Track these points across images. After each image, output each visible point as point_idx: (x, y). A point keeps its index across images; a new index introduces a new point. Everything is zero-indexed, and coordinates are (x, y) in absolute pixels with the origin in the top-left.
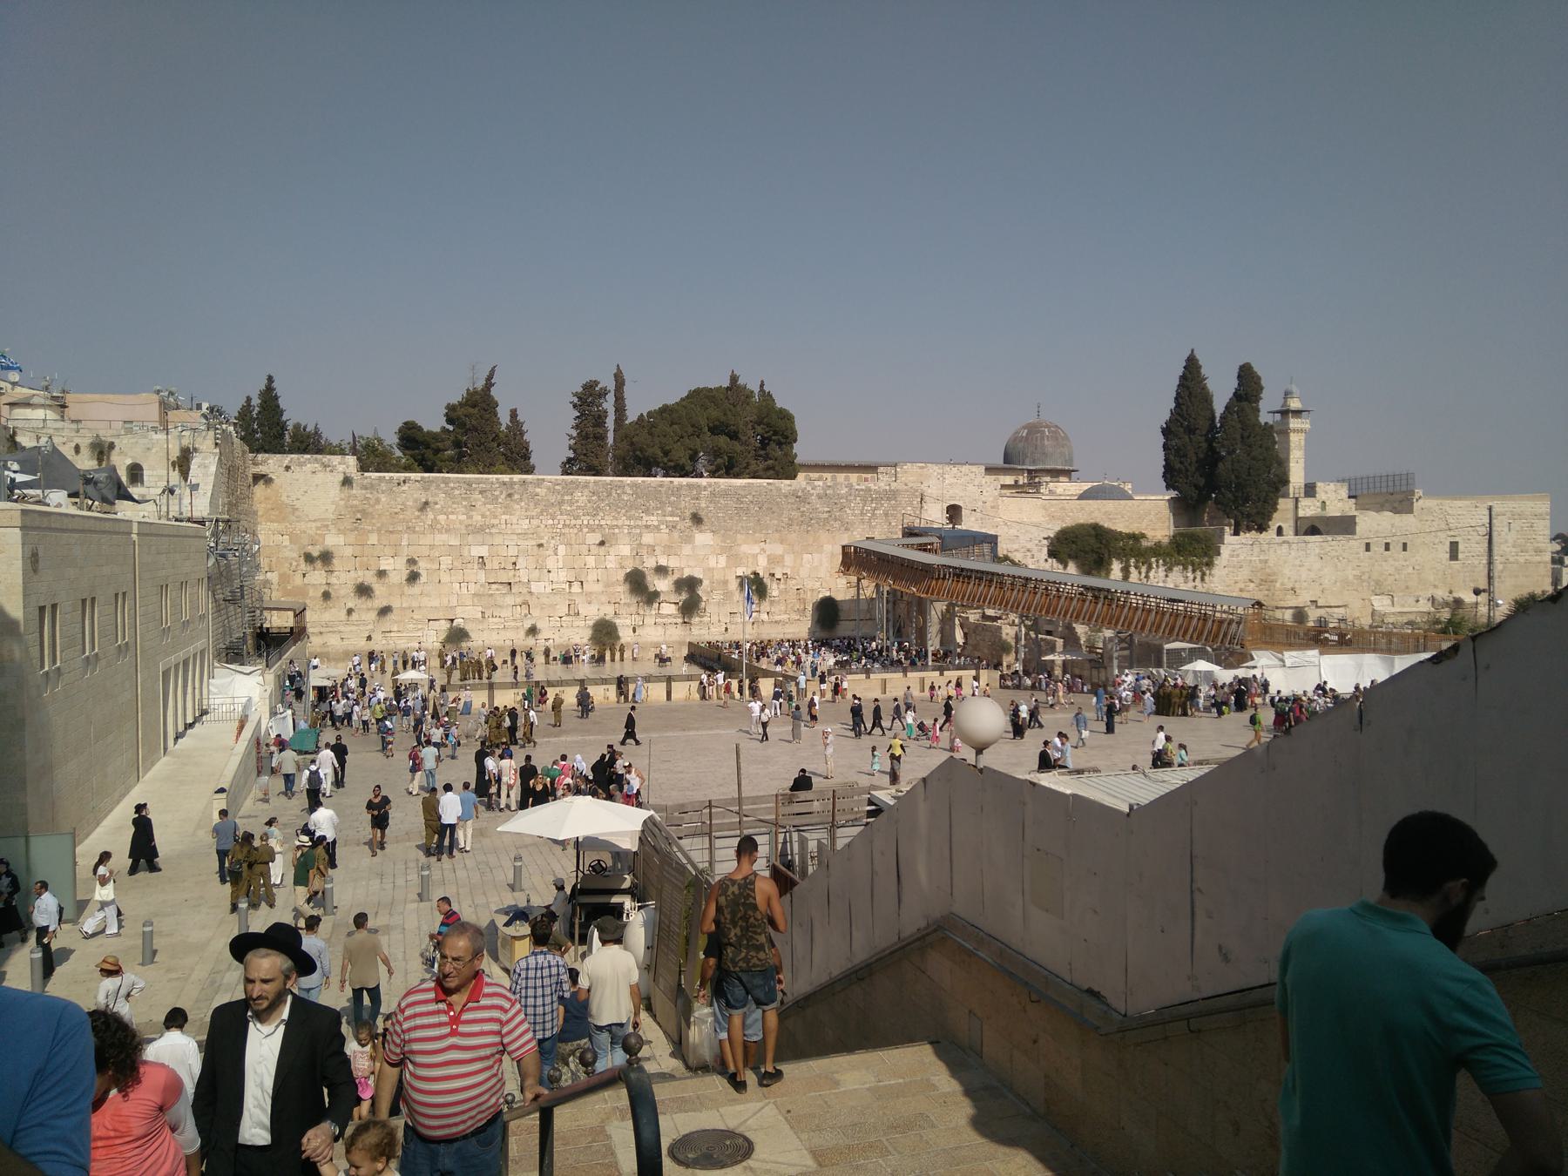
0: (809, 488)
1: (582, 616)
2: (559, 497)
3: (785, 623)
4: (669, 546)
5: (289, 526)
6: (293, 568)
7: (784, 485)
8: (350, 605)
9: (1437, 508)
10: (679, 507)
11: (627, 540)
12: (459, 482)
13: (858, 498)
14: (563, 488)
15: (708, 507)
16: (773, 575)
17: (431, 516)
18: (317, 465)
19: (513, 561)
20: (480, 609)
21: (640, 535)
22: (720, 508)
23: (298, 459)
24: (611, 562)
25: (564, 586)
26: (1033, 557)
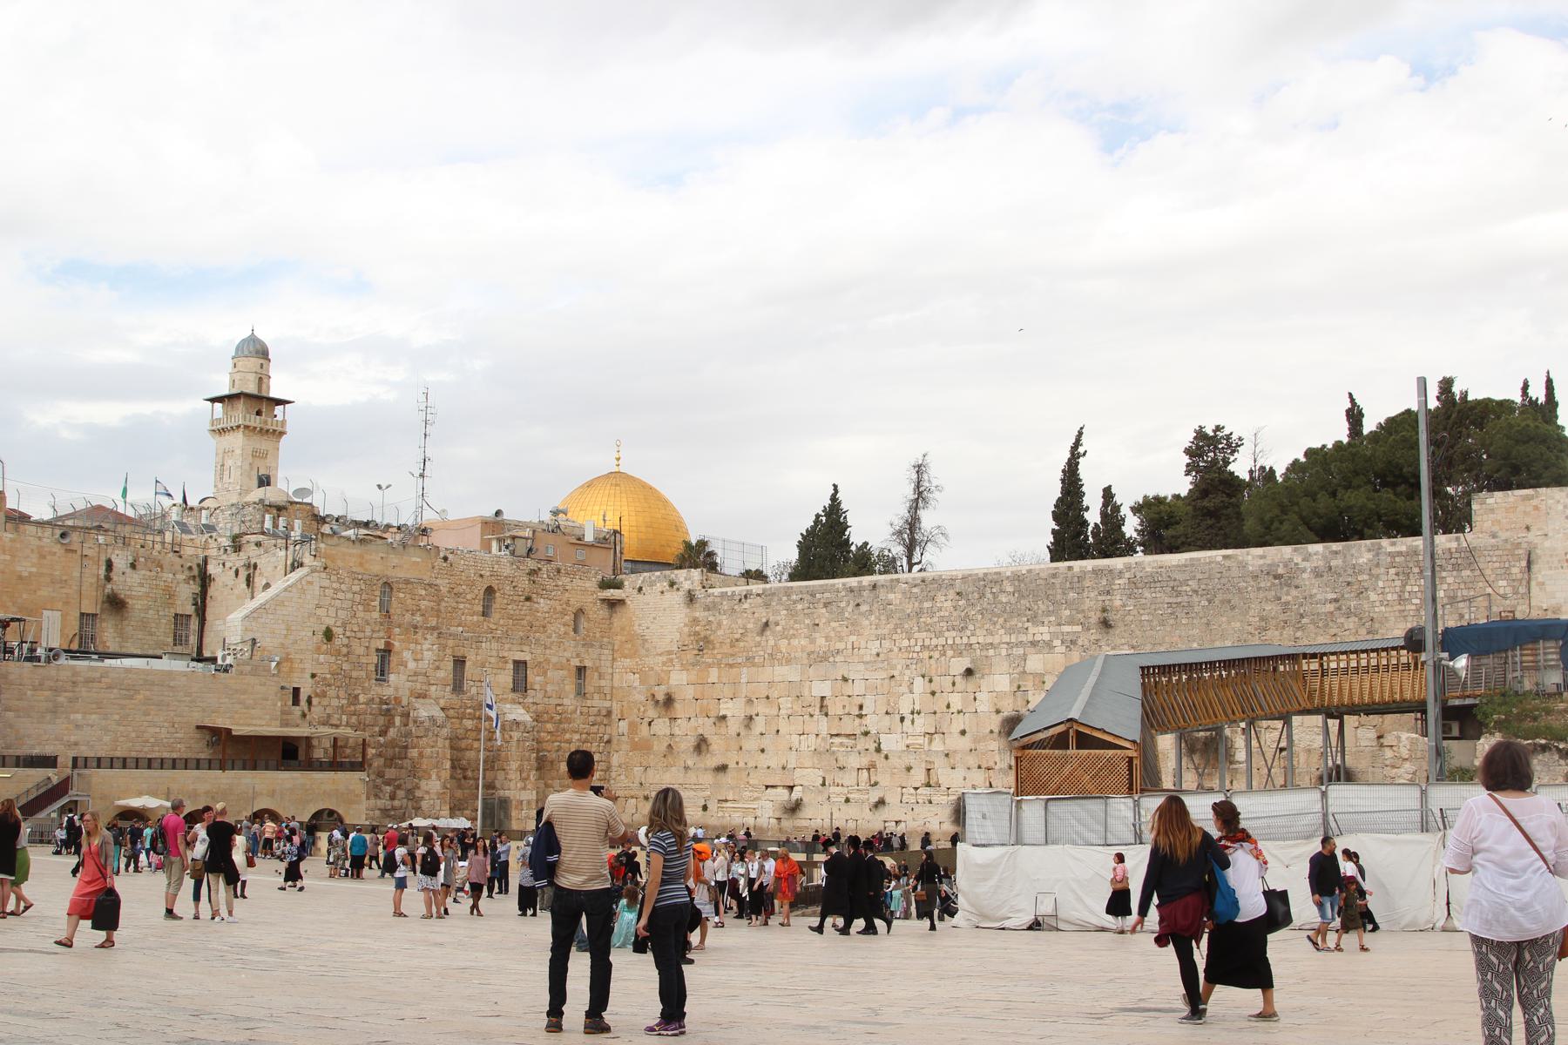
0: (1298, 559)
1: (943, 788)
2: (917, 604)
7: (1253, 557)
10: (1082, 607)
11: (1006, 664)
13: (1392, 571)
15: (1124, 606)
17: (771, 643)
20: (821, 773)
22: (1144, 607)
23: (650, 577)
24: (984, 704)
25: (920, 740)
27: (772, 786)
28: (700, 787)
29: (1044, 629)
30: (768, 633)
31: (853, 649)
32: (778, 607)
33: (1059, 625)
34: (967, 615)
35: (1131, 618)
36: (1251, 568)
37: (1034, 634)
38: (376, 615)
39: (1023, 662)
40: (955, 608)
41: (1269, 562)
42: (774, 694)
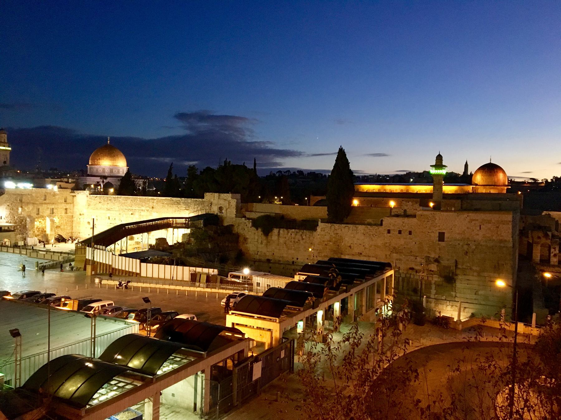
9: (430, 216)
26: (246, 225)
29: (144, 208)
38: (19, 202)
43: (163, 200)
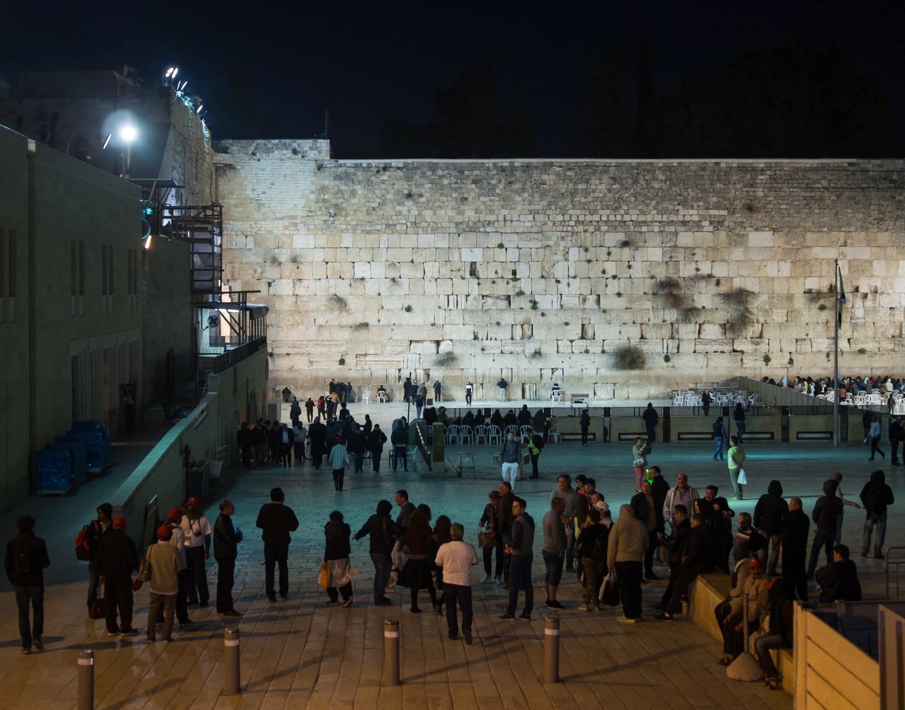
2: (571, 186)
3: (873, 354)
4: (713, 249)
5: (254, 226)
6: (257, 276)
8: (321, 321)
10: (728, 195)
11: (658, 240)
12: (448, 168)
14: (576, 174)
15: (766, 196)
16: (857, 289)
18: (285, 152)
19: (514, 269)
20: (471, 328)
21: (676, 234)
24: (639, 270)
27: (417, 341)
28: (332, 343)
29: (694, 212)
30: (409, 203)
31: (505, 221)
32: (421, 181)
33: (708, 209)
34: (621, 198)
35: (772, 206)
36: (871, 174)
37: (684, 216)
39: (675, 238)
40: (609, 191)
41: (885, 168)
42: (418, 259)
43: (805, 170)
